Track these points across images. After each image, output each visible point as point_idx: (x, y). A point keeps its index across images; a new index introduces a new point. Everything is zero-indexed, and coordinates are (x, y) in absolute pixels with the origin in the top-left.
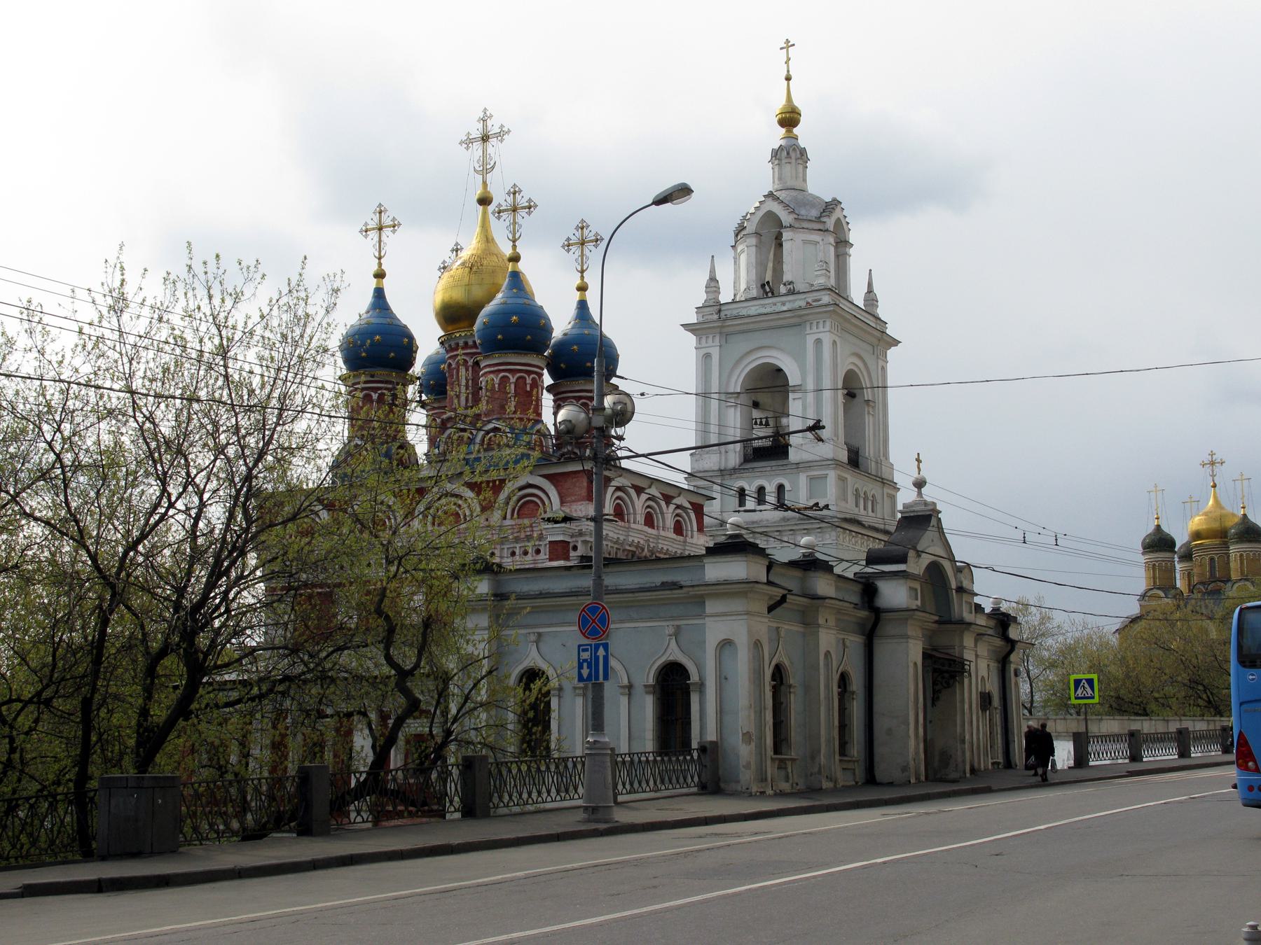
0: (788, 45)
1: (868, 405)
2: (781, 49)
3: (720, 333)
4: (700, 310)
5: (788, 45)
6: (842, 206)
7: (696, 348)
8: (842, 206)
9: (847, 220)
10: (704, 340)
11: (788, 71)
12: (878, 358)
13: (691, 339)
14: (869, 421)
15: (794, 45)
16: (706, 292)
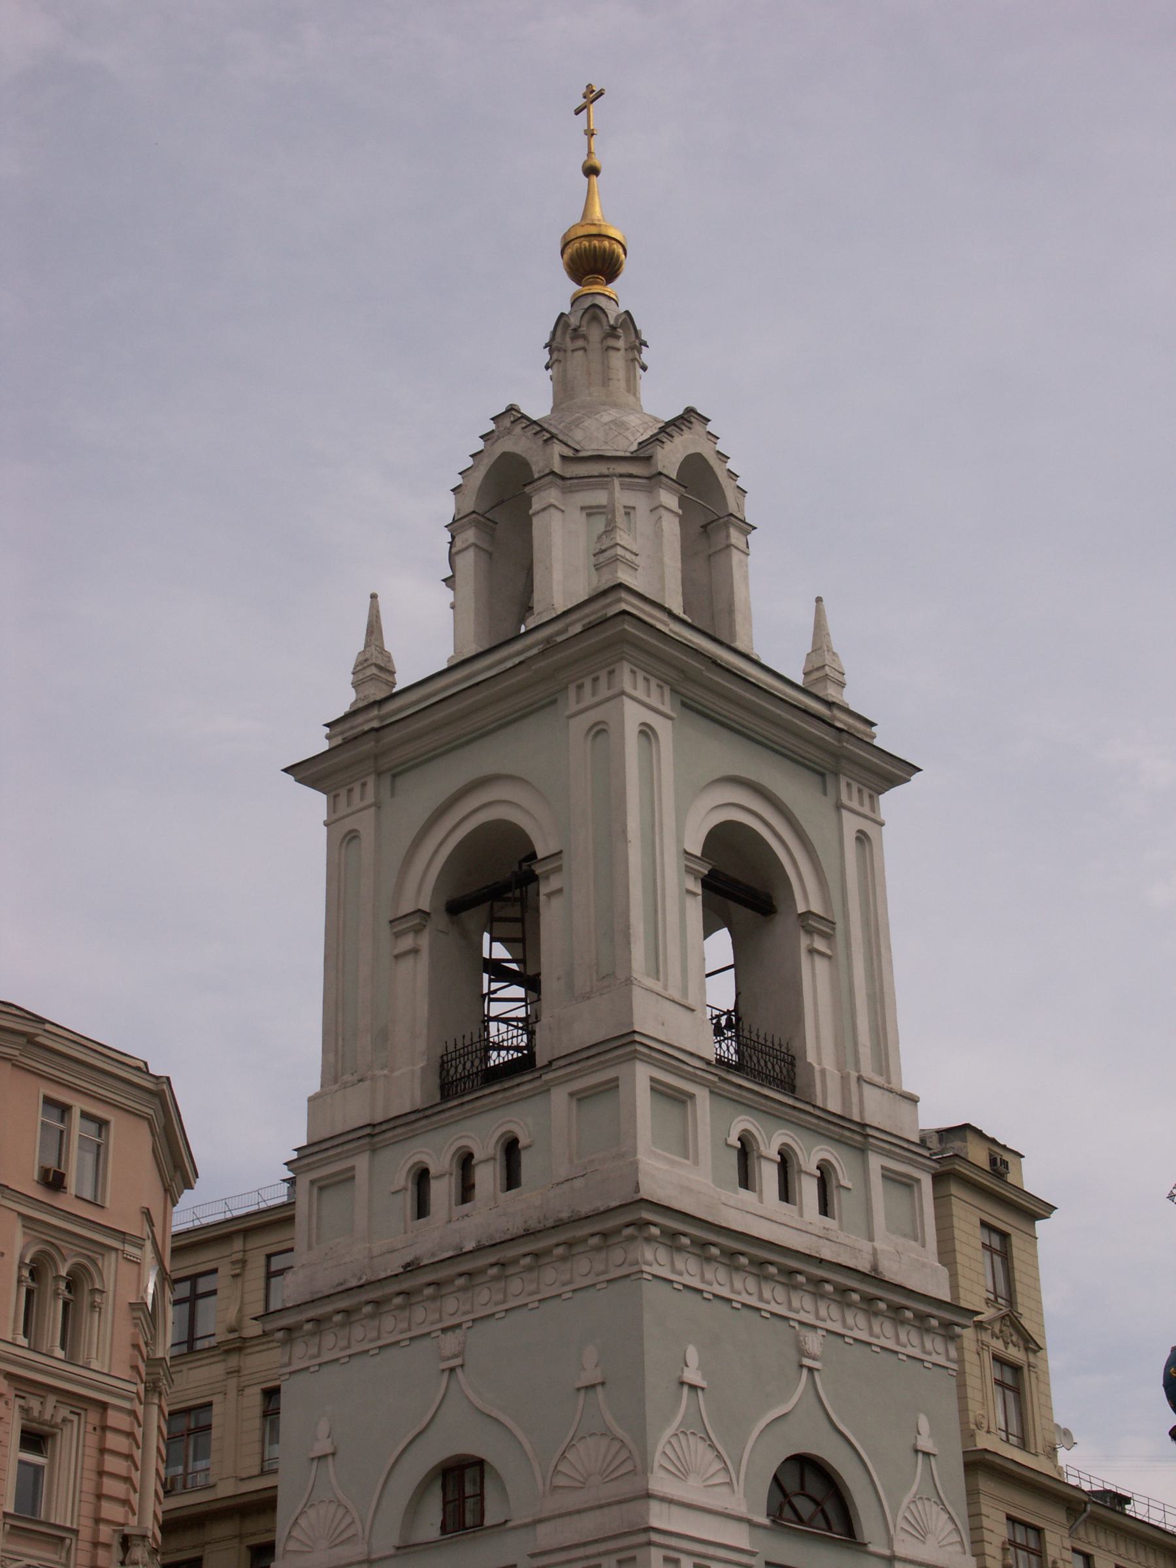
0: (593, 95)
1: (810, 932)
2: (577, 112)
3: (379, 774)
4: (338, 729)
5: (593, 95)
6: (710, 427)
7: (326, 824)
8: (710, 427)
9: (730, 465)
10: (343, 799)
11: (590, 153)
12: (839, 806)
13: (316, 802)
15: (601, 94)
16: (356, 685)
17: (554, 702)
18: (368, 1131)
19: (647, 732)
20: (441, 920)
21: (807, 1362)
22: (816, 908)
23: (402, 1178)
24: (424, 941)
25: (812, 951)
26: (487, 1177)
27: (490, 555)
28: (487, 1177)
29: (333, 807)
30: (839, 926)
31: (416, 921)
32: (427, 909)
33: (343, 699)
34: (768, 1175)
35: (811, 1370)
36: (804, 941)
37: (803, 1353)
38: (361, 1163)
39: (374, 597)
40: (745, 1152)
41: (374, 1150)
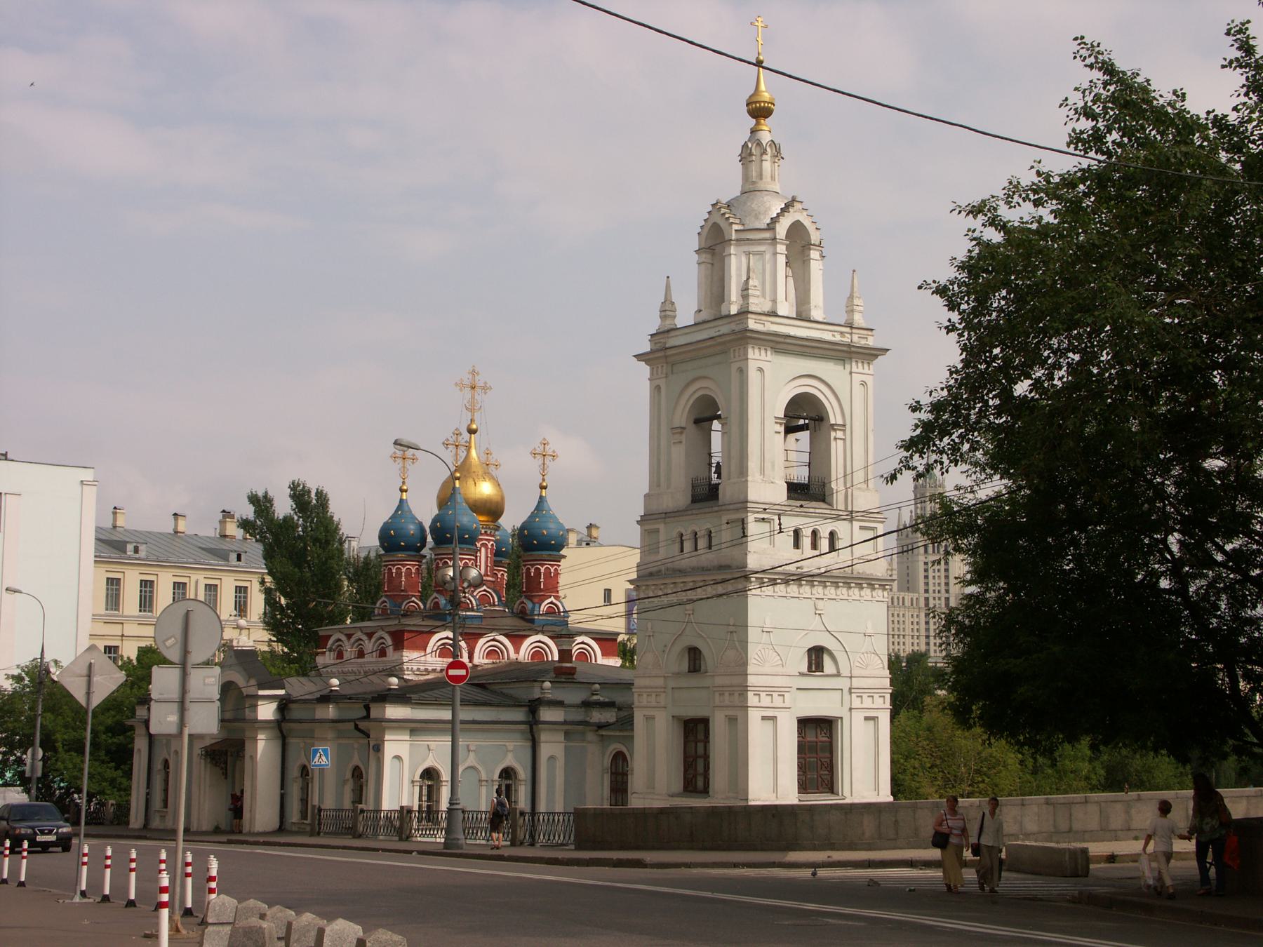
1: (835, 430)
13: (644, 369)
14: (836, 449)
17: (725, 352)
18: (663, 515)
19: (760, 369)
20: (692, 428)
21: (817, 612)
22: (840, 422)
23: (675, 534)
24: (683, 438)
25: (836, 439)
26: (702, 543)
27: (712, 264)
28: (702, 543)
29: (652, 374)
30: (848, 427)
31: (679, 430)
32: (683, 425)
33: (654, 325)
34: (806, 541)
35: (820, 614)
36: (833, 434)
37: (816, 609)
38: (661, 527)
39: (668, 277)
40: (797, 534)
41: (665, 523)
